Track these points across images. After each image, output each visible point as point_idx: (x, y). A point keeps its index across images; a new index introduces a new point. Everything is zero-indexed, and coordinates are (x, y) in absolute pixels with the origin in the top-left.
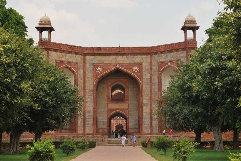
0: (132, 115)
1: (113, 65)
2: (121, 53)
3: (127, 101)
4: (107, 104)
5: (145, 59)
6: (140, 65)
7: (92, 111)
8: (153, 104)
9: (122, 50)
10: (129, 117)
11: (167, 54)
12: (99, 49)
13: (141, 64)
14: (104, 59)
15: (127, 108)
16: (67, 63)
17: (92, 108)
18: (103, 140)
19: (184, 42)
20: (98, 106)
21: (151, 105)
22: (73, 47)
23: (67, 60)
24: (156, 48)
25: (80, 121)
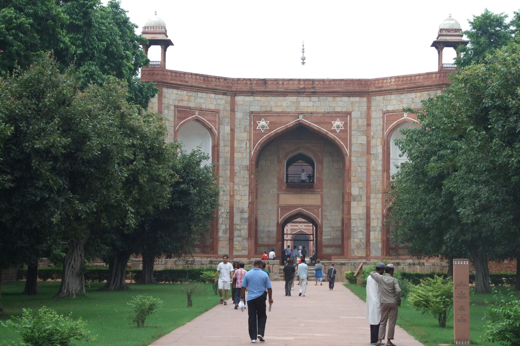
0: (329, 218)
1: (291, 116)
2: (307, 92)
4: (278, 195)
8: (372, 196)
9: (310, 86)
10: (322, 221)
11: (402, 96)
12: (263, 82)
13: (349, 113)
14: (272, 103)
15: (319, 203)
16: (197, 113)
17: (247, 203)
19: (436, 73)
22: (210, 79)
23: (197, 106)
24: (381, 81)
25: (223, 230)
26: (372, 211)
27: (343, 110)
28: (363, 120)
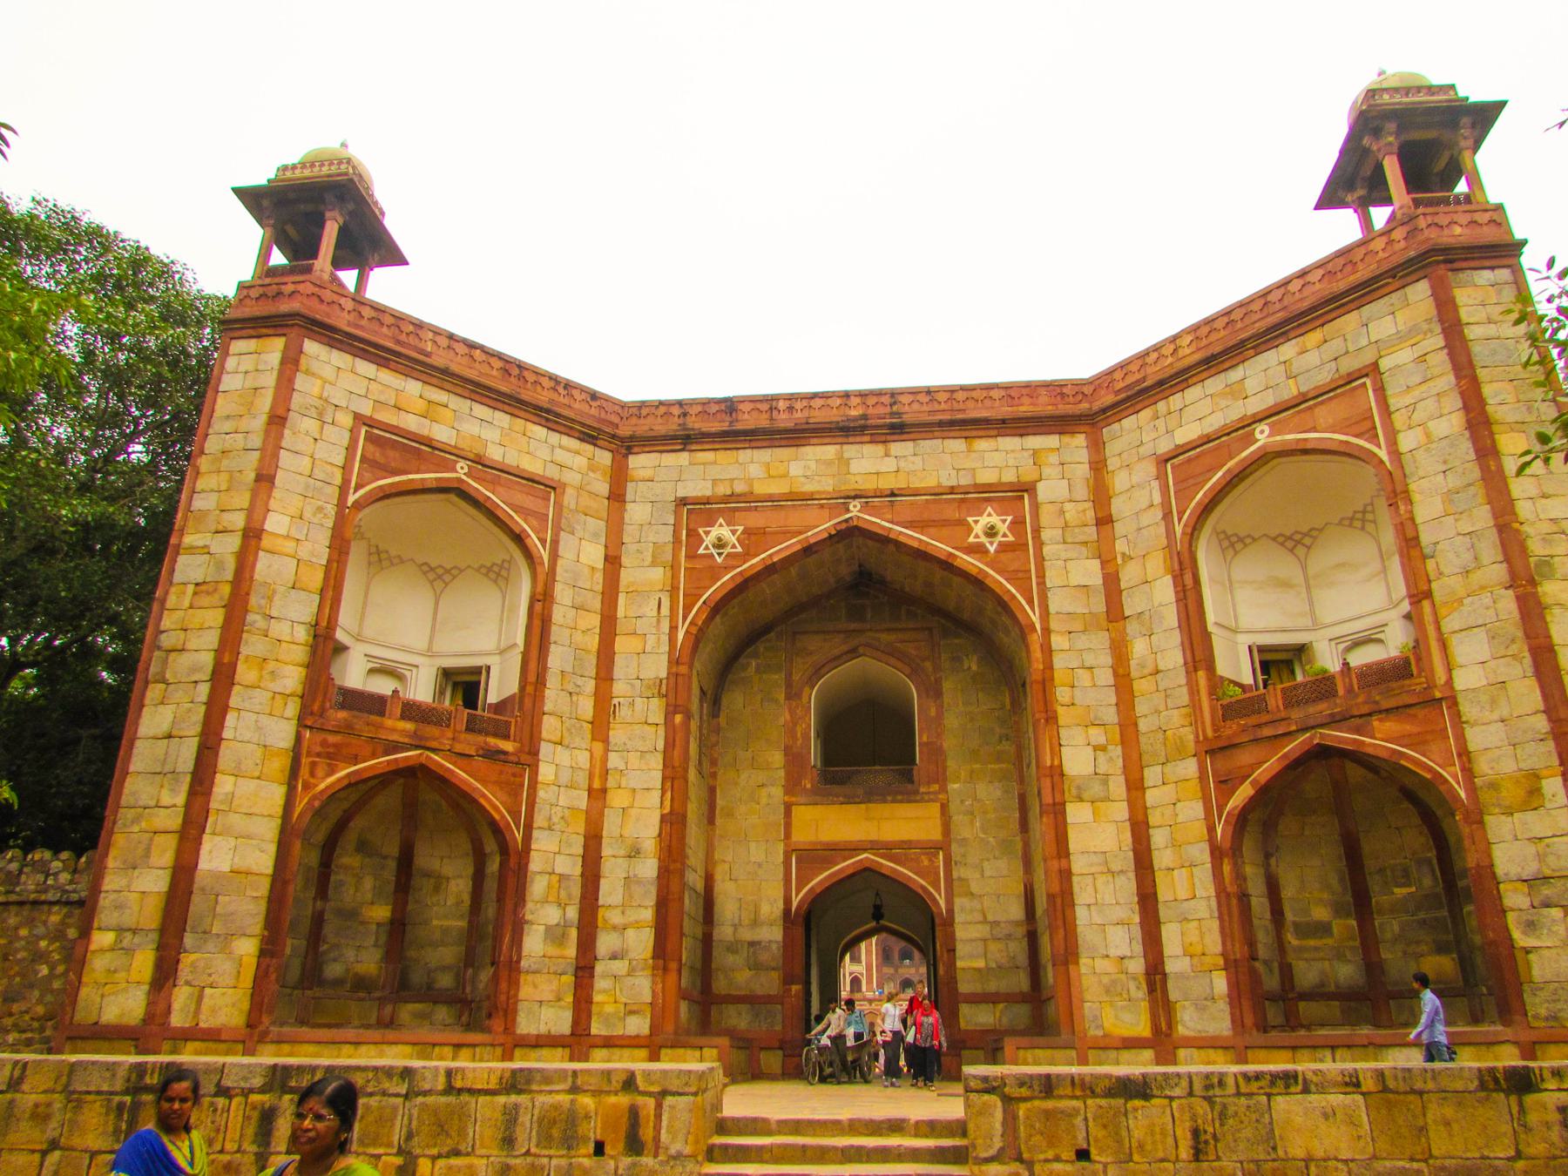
0: (975, 888)
1: (822, 506)
3: (929, 783)
5: (1054, 458)
6: (1022, 498)
7: (650, 845)
8: (1152, 775)
9: (881, 410)
10: (950, 902)
11: (1235, 375)
13: (1028, 488)
14: (755, 470)
15: (936, 835)
16: (462, 468)
18: (634, 1113)
20: (718, 821)
21: (1135, 786)
22: (531, 378)
26: (1158, 838)
27: (1004, 480)
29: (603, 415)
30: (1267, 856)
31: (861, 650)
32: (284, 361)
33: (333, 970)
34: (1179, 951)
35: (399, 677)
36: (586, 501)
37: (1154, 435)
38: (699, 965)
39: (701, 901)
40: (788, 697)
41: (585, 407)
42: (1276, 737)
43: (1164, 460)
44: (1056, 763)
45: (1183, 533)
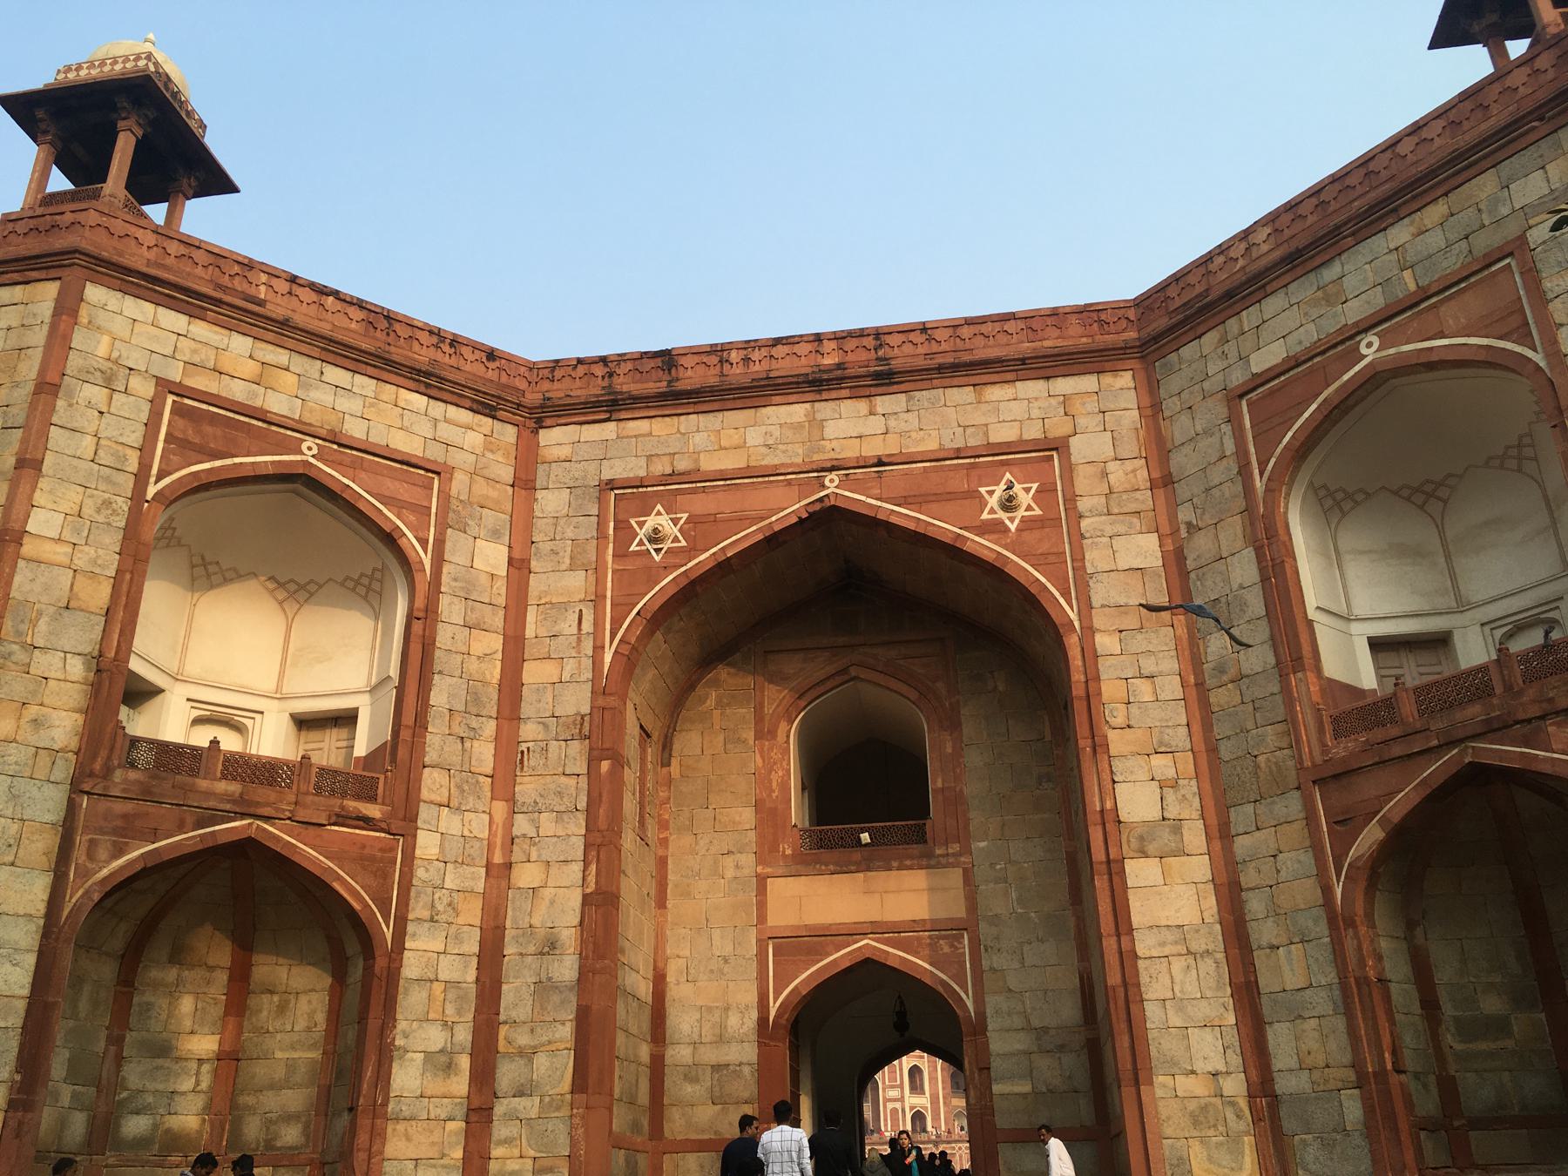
0: (1013, 982)
1: (789, 483)
3: (946, 844)
4: (762, 881)
5: (1092, 405)
7: (569, 936)
8: (1241, 817)
9: (863, 356)
11: (1329, 274)
13: (1059, 446)
14: (699, 440)
15: (959, 910)
20: (669, 904)
21: (1221, 834)
22: (403, 331)
23: (307, 418)
25: (428, 1055)
26: (1255, 905)
27: (1025, 437)
28: (1129, 465)
29: (504, 379)
30: (1410, 925)
31: (853, 672)
32: (58, 312)
33: (135, 1126)
34: (1294, 1063)
35: (238, 728)
36: (481, 488)
37: (1225, 364)
38: (644, 1097)
39: (647, 1012)
40: (759, 736)
41: (479, 369)
42: (1409, 756)
43: (1235, 397)
44: (1109, 805)
45: (1268, 490)
